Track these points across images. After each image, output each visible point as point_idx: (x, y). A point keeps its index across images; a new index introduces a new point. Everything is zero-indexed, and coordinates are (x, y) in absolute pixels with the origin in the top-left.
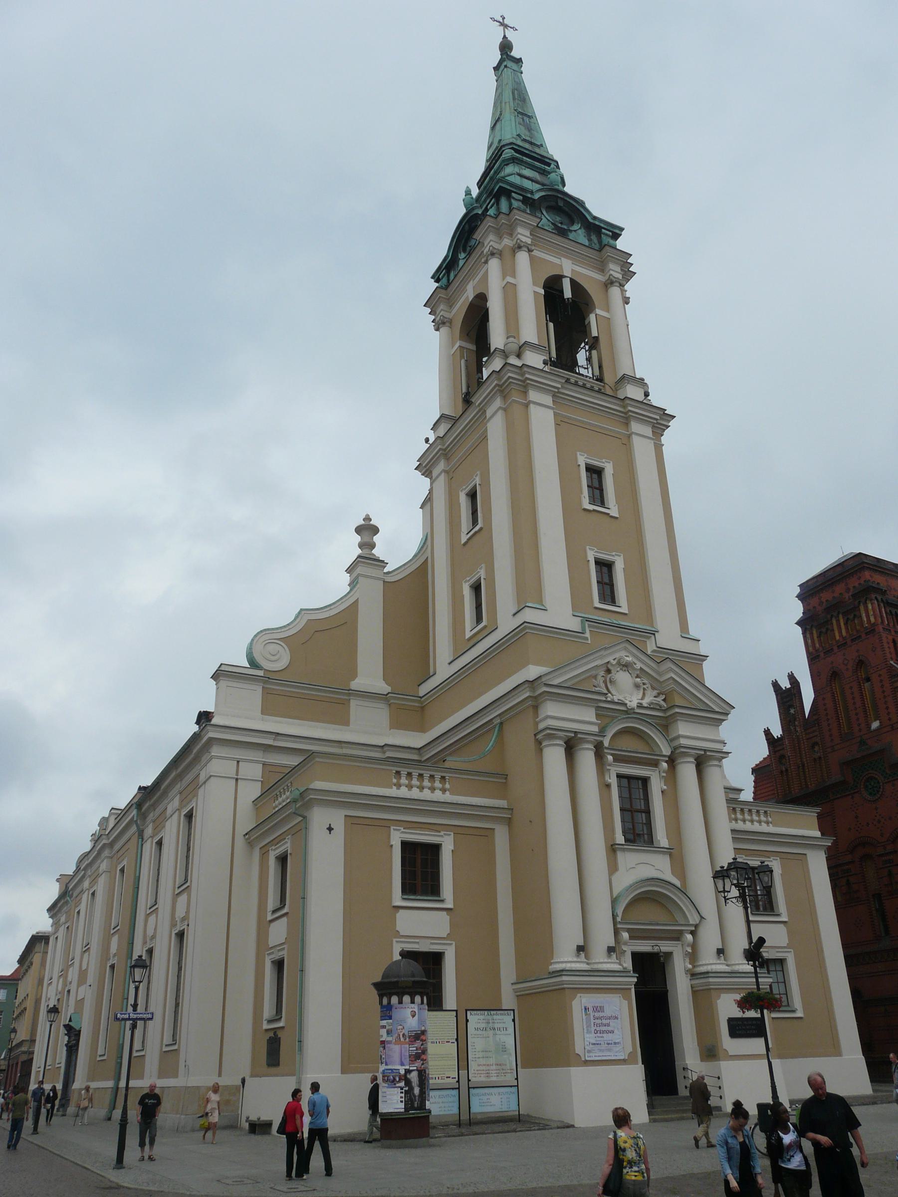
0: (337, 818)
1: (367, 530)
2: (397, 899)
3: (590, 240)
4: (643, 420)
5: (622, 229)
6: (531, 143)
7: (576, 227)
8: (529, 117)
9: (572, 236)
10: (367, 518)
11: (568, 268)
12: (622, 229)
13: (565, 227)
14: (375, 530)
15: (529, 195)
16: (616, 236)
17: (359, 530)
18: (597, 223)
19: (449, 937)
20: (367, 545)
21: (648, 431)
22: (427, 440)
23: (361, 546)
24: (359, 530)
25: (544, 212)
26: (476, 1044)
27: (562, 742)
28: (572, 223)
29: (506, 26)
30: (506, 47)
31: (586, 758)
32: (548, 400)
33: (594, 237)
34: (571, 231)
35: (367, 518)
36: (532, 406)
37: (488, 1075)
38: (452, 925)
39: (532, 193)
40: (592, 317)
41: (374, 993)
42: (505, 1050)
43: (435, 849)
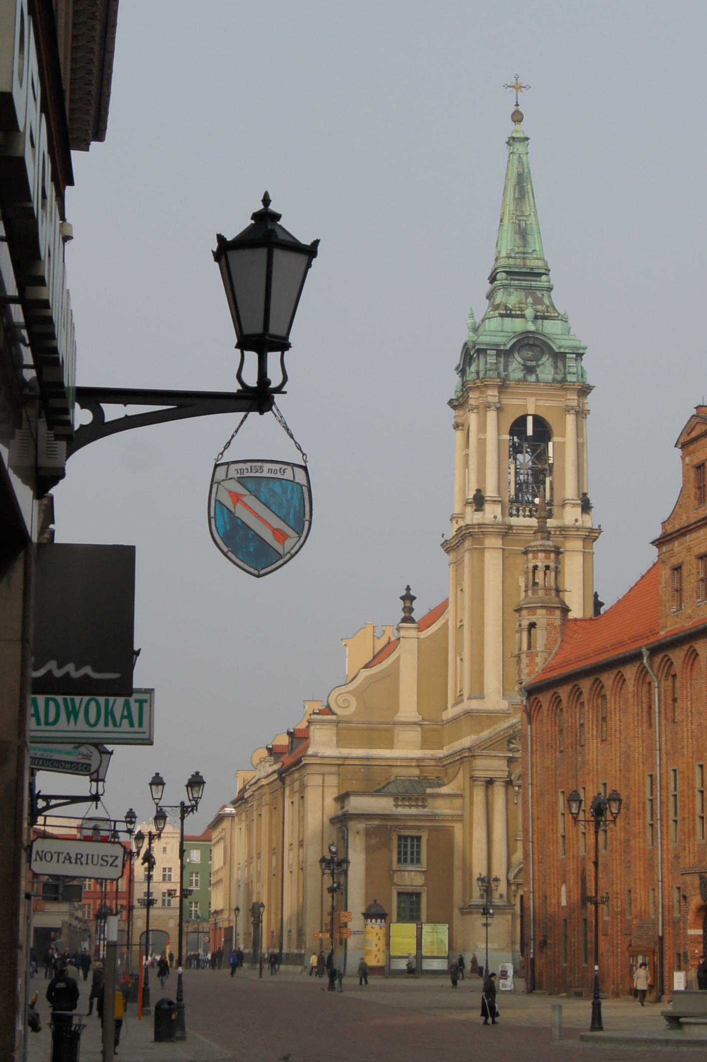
0: (361, 826)
1: (408, 598)
2: (395, 866)
3: (556, 367)
4: (576, 537)
5: (585, 348)
6: (524, 253)
7: (544, 359)
8: (527, 216)
9: (539, 370)
10: (408, 589)
11: (531, 406)
12: (585, 348)
13: (534, 363)
14: (413, 598)
15: (502, 348)
16: (579, 356)
17: (403, 598)
18: (562, 350)
19: (423, 886)
20: (409, 610)
21: (578, 544)
22: (443, 536)
23: (404, 609)
24: (403, 598)
25: (516, 356)
26: (426, 939)
27: (483, 783)
28: (542, 353)
29: (518, 87)
30: (517, 117)
31: (499, 792)
32: (497, 542)
33: (560, 364)
34: (538, 366)
35: (408, 589)
36: (486, 551)
37: (432, 952)
38: (426, 879)
39: (505, 345)
40: (550, 444)
41: (362, 917)
42: (442, 942)
43: (419, 838)
